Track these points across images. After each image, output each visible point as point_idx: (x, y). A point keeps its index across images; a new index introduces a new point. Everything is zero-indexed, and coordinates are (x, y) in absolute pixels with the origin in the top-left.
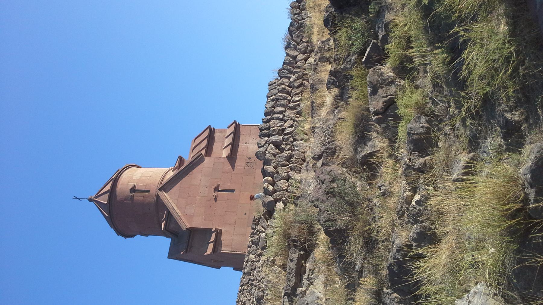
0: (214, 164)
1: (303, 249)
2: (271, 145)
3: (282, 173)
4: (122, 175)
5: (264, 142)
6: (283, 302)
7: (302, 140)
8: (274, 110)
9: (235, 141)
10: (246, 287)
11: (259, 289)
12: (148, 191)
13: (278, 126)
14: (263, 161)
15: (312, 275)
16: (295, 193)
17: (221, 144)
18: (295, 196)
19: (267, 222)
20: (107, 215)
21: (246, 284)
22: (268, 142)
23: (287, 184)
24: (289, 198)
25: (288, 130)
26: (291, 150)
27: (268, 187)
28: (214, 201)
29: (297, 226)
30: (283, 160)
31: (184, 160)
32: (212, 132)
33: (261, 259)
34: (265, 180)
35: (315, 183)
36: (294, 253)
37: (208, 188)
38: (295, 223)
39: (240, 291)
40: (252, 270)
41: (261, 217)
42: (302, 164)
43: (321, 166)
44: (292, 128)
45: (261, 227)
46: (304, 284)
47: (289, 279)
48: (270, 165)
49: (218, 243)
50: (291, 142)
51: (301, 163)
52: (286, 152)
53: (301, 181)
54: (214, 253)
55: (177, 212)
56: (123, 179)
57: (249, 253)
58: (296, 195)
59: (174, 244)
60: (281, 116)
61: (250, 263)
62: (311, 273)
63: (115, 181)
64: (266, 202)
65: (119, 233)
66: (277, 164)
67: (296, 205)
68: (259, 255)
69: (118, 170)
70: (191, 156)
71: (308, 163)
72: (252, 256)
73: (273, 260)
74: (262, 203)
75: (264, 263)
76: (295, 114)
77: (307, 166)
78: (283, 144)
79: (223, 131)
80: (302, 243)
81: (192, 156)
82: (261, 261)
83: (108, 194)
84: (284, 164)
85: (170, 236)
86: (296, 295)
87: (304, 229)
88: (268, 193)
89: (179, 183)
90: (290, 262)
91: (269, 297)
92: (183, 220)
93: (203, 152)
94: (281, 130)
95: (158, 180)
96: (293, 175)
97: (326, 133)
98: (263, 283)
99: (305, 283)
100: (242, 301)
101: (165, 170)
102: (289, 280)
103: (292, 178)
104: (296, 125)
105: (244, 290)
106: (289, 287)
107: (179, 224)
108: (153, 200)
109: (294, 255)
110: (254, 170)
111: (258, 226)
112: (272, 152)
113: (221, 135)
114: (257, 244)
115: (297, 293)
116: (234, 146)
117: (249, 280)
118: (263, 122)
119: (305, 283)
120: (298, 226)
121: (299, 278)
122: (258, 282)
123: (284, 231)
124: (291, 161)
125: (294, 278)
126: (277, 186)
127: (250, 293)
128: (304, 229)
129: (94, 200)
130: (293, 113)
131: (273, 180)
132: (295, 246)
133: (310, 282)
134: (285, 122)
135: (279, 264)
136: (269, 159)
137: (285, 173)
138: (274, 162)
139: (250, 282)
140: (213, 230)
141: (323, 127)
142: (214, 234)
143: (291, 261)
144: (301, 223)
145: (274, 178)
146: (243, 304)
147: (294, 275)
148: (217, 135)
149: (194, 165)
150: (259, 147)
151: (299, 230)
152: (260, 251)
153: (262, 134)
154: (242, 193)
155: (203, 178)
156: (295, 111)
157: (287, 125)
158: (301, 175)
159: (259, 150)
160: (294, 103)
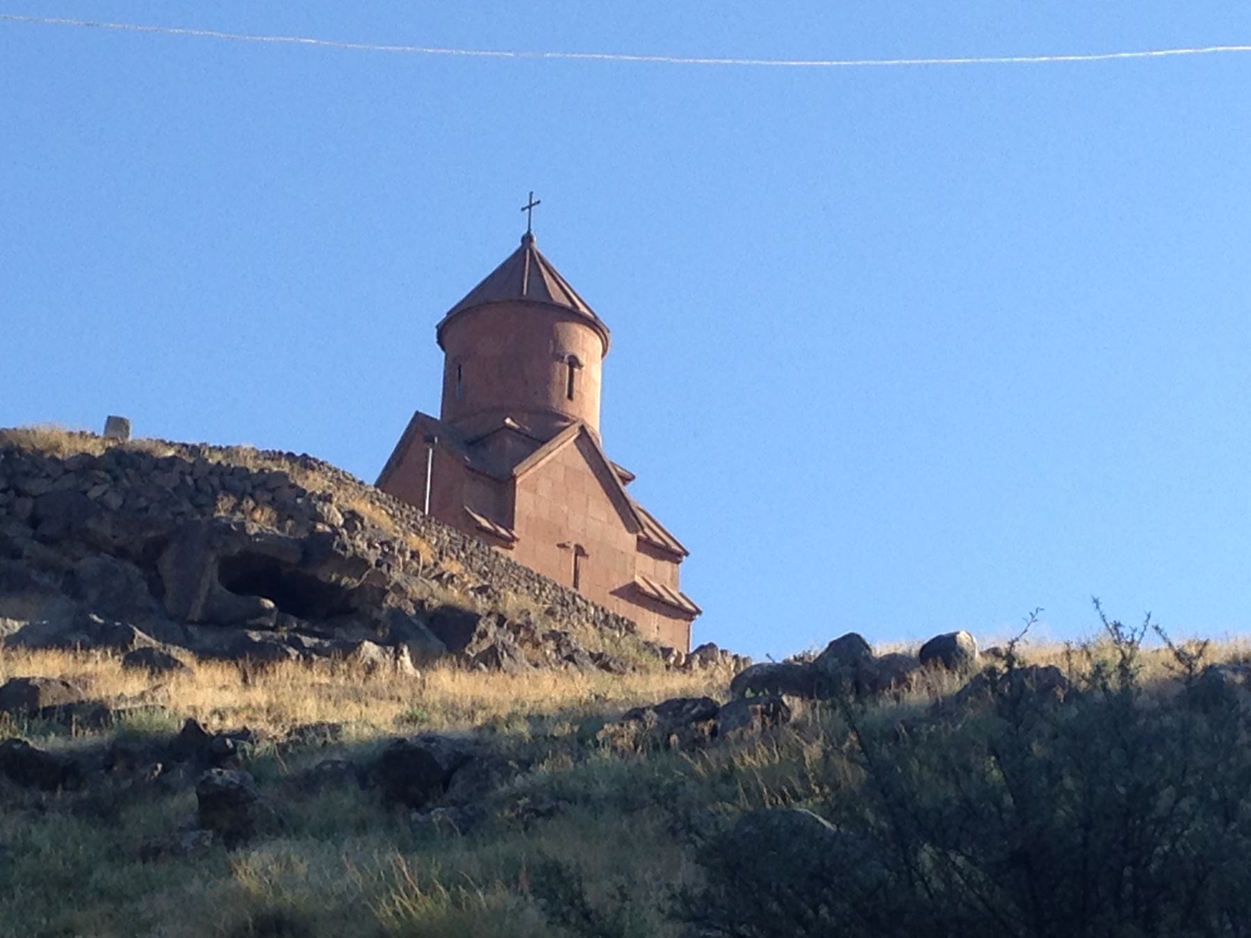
0: (622, 553)
12: (570, 397)
27: (674, 655)
31: (624, 484)
33: (589, 626)
54: (477, 528)
57: (596, 608)
63: (593, 324)
68: (594, 624)
69: (609, 331)
72: (592, 611)
95: (590, 424)
100: (546, 585)
108: (555, 406)
116: (657, 603)
139: (565, 603)
148: (666, 566)
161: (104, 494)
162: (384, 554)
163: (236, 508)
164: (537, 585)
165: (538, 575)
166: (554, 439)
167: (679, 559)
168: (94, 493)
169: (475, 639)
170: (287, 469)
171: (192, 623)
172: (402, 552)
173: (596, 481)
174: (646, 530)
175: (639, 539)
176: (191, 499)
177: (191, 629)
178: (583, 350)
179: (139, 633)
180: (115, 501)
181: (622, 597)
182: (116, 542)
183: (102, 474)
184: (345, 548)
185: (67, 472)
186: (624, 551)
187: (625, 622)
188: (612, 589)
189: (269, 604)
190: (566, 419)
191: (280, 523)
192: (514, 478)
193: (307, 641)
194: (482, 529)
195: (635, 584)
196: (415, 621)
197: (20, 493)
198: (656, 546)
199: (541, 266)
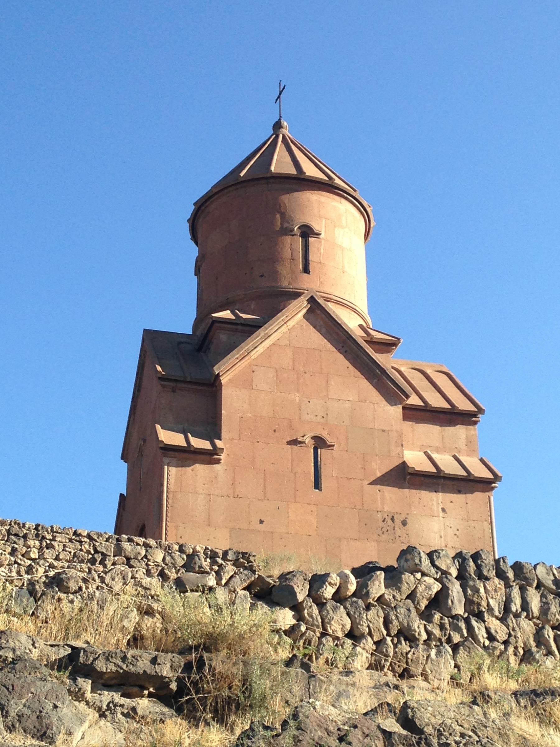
0: (383, 431)
1: (182, 690)
2: (437, 587)
3: (367, 619)
4: (343, 201)
5: (444, 567)
6: (58, 646)
7: (456, 666)
8: (531, 585)
9: (447, 482)
10: (87, 546)
11: (85, 580)
12: (306, 270)
13: (488, 604)
14: (396, 566)
15: (122, 713)
16: (317, 658)
17: (437, 445)
18: (310, 659)
19: (244, 589)
20: (242, 174)
21: (94, 545)
22: (447, 578)
23: (340, 634)
24: (305, 640)
25: (479, 628)
26: (429, 639)
27: (330, 584)
28: (289, 439)
29: (238, 669)
30: (401, 619)
33: (154, 582)
34: (347, 576)
35: (340, 718)
36: (171, 667)
37: (322, 420)
38: (245, 663)
39: (78, 532)
40: (128, 559)
41: (254, 572)
42: (393, 670)
43: (384, 732)
44: (488, 638)
45: (231, 574)
46: (100, 694)
47: (112, 657)
48: (386, 587)
50: (449, 640)
51: (396, 667)
52: (422, 627)
53: (348, 672)
54: (161, 448)
55: (258, 349)
56: (334, 203)
57: (168, 549)
58: (312, 662)
59: (180, 343)
60: (516, 606)
61: (143, 552)
62: (126, 711)
64: (292, 584)
65: (202, 205)
66: (389, 605)
67: (289, 663)
68: (163, 575)
69: (355, 191)
70: (403, 365)
71: (396, 687)
72: (159, 556)
73: (152, 608)
74: (289, 573)
75: (146, 589)
76: (525, 644)
77: (387, 685)
78: (442, 618)
80: (195, 684)
81: (403, 369)
82: (149, 579)
83: (296, 173)
84: (392, 623)
85: (198, 333)
86: (73, 677)
87: (230, 688)
88: (315, 587)
89: (329, 345)
90: (150, 657)
91: (65, 604)
92: (239, 364)
93: (414, 400)
94: (478, 608)
95: (337, 292)
96: (364, 649)
97: (470, 736)
98: (97, 588)
99: (103, 698)
100: (54, 539)
101: (362, 305)
102: (108, 657)
103: (355, 646)
104: (494, 648)
105: (81, 542)
106: (91, 659)
107: (229, 356)
108: (285, 284)
109: (168, 665)
110: (376, 537)
111: (234, 565)
112: (421, 588)
113: (462, 444)
115: (79, 679)
117: (103, 554)
118: (497, 562)
119: (103, 698)
120: (238, 670)
121: (113, 682)
122: (99, 577)
123: (223, 636)
124: (399, 642)
125: (114, 669)
126: (335, 609)
127: (73, 558)
128: (230, 688)
129: (277, 136)
130: (528, 639)
131: (350, 597)
132: (188, 667)
133: (106, 710)
134: (503, 620)
135: (145, 628)
136: (400, 581)
137: (368, 626)
138: (394, 597)
139: (98, 557)
140: (217, 442)
141: (486, 727)
142: (205, 445)
143: (154, 661)
144: (244, 681)
145: (355, 599)
146: (48, 542)
147: (122, 668)
149: (378, 380)
150: (430, 555)
151: (227, 676)
152: (173, 575)
153: (464, 559)
154: (314, 508)
155: (347, 405)
156: (533, 644)
157: (494, 624)
158: (365, 671)
159: (422, 554)
160: (555, 640)
164: (34, 543)
165: (37, 526)
166: (271, 321)
167: (474, 419)
173: (341, 357)
178: (320, 217)
181: (388, 485)
186: (386, 428)
187: (231, 556)
188: (374, 479)
195: (404, 465)
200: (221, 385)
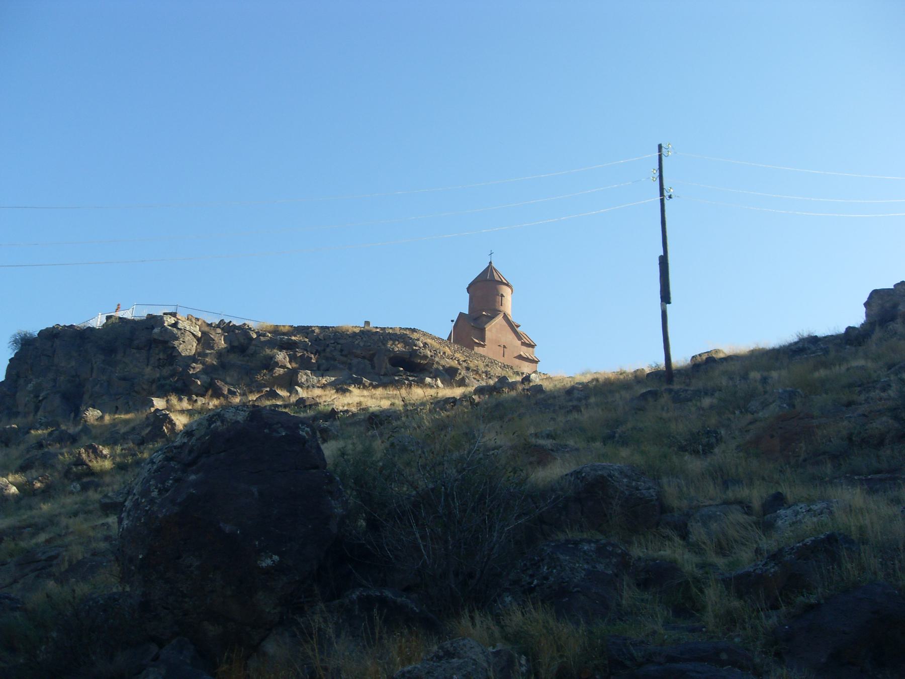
12: (501, 305)
20: (488, 278)
31: (517, 328)
32: (533, 346)
41: (513, 369)
49: (479, 345)
57: (501, 363)
63: (507, 285)
68: (501, 368)
72: (500, 364)
79: (533, 353)
108: (497, 308)
113: (531, 352)
114: (504, 367)
116: (527, 359)
148: (530, 349)
161: (359, 342)
162: (435, 354)
163: (393, 344)
168: (357, 342)
169: (458, 375)
170: (407, 333)
171: (382, 375)
172: (440, 353)
173: (509, 328)
174: (525, 339)
175: (522, 342)
176: (382, 342)
177: (382, 377)
179: (364, 379)
180: (362, 344)
182: (362, 355)
183: (359, 337)
184: (421, 353)
185: (350, 337)
189: (402, 369)
190: (500, 311)
191: (405, 347)
192: (485, 328)
193: (411, 378)
194: (477, 343)
195: (521, 355)
196: (442, 371)
197: (338, 344)
198: (527, 344)
199: (494, 271)
200: (485, 330)
